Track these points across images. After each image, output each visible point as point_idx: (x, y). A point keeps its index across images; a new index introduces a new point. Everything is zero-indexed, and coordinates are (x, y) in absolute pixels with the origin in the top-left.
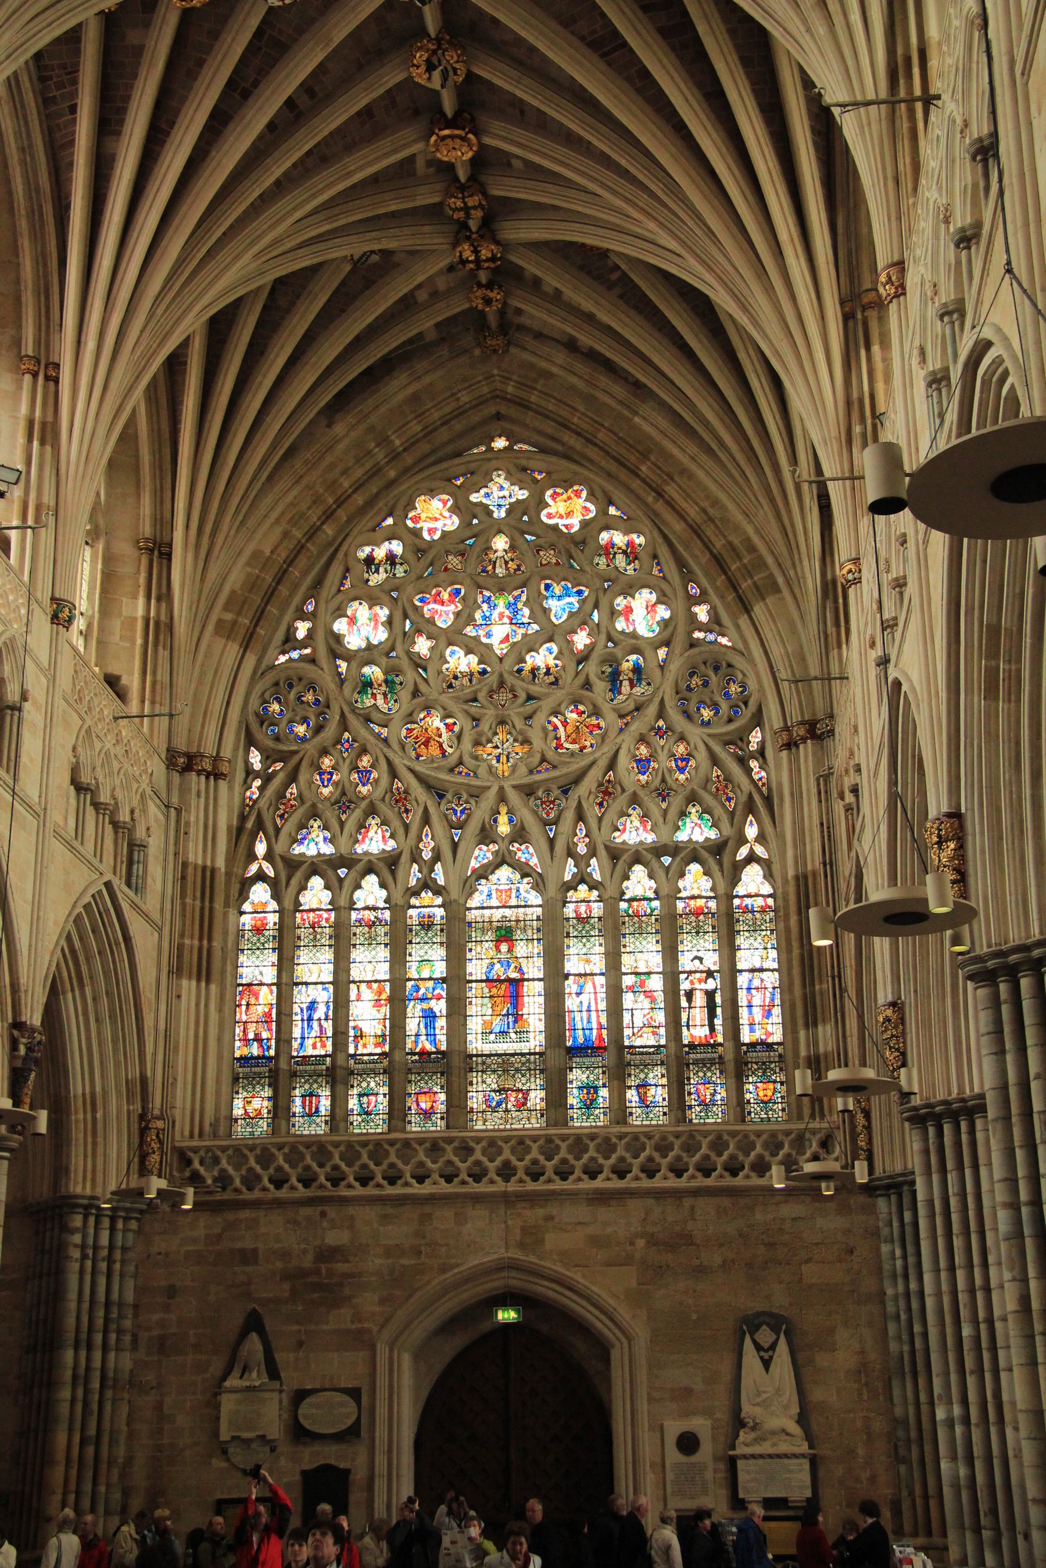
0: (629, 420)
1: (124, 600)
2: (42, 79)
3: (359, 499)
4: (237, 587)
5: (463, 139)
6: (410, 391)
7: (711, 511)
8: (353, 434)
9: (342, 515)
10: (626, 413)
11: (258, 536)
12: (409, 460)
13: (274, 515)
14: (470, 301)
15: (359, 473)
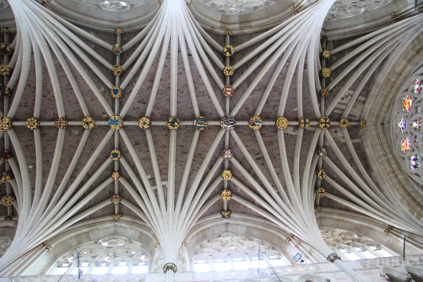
0: (381, 86)
1: (398, 245)
2: (246, 214)
3: (395, 166)
4: (408, 209)
5: (279, 120)
6: (370, 148)
7: (403, 57)
8: (377, 165)
9: (397, 172)
10: (379, 86)
11: (396, 199)
12: (387, 150)
13: (392, 192)
14: (344, 128)
15: (387, 165)
